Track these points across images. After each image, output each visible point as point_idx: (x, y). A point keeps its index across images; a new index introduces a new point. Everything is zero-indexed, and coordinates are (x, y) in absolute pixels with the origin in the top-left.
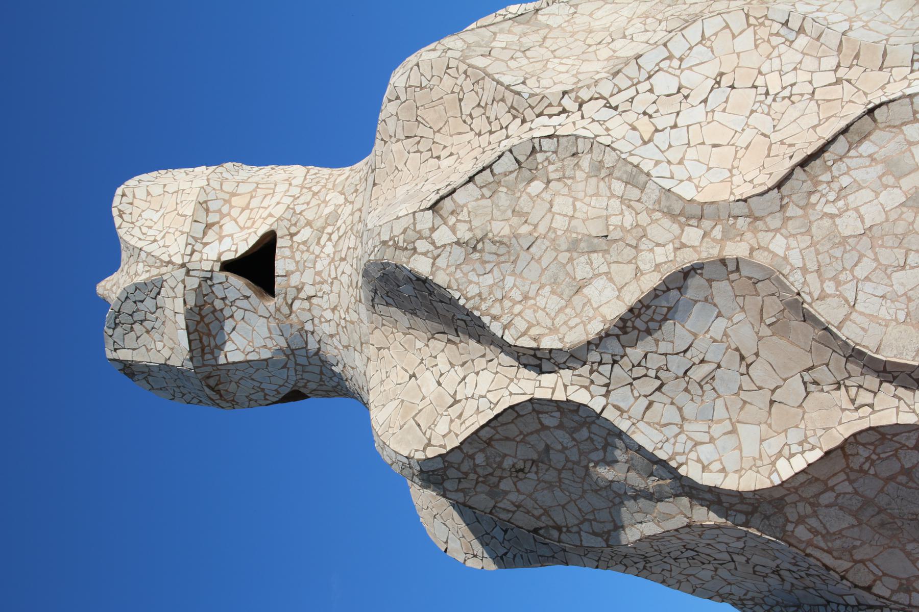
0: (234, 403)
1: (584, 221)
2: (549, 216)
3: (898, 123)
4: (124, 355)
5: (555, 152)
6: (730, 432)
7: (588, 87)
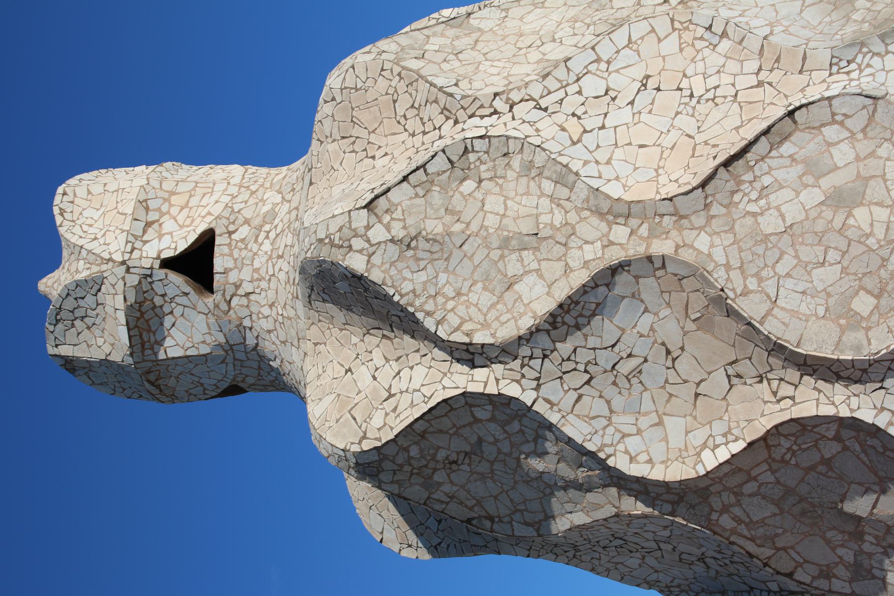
0: (173, 398)
1: (515, 219)
2: (481, 214)
3: (817, 124)
4: (65, 351)
5: (487, 152)
6: (657, 425)
7: (519, 89)
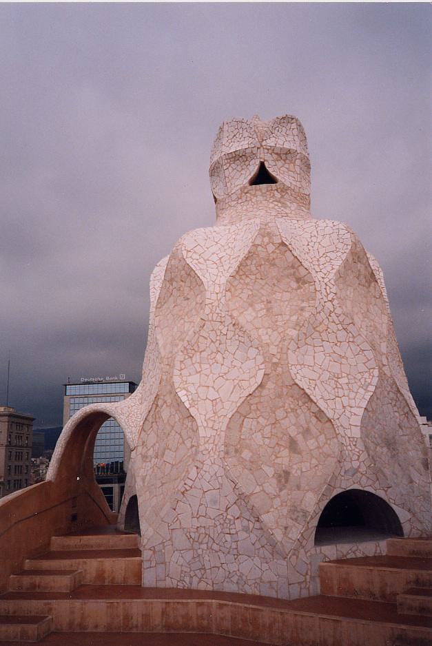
0: (211, 176)
